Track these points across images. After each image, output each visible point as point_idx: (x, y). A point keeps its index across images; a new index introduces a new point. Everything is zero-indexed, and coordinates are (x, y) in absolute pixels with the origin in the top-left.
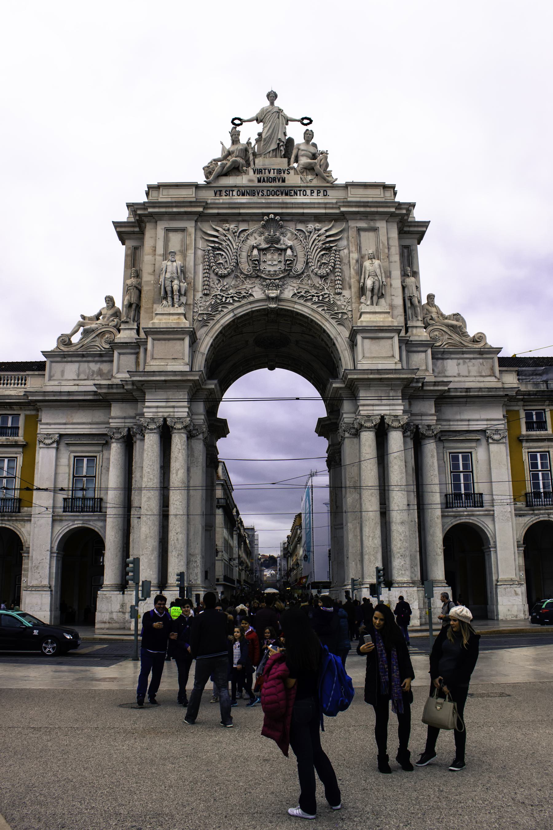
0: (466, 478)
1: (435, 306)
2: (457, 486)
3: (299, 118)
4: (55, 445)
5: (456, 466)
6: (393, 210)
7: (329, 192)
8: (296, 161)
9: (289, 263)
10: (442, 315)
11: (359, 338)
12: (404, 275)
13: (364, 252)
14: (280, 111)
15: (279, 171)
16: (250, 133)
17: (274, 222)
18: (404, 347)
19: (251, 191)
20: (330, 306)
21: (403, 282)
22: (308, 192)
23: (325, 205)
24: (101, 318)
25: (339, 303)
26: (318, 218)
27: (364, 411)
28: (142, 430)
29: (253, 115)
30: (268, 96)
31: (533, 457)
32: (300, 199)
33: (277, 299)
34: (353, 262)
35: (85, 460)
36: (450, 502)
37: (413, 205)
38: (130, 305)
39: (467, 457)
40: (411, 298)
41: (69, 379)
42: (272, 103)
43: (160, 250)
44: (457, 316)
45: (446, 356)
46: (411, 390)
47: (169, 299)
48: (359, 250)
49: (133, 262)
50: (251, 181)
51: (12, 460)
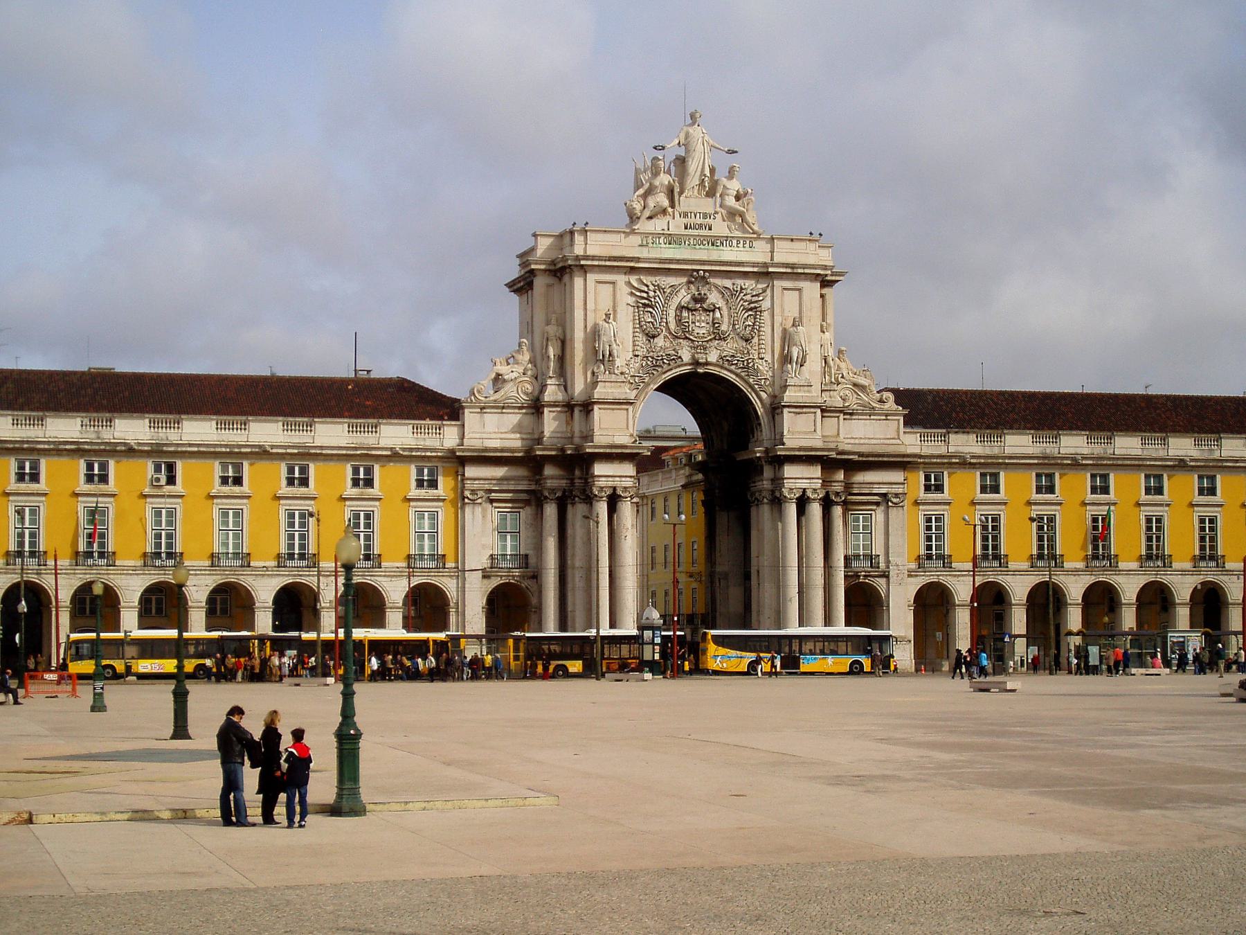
15: (705, 216)
22: (735, 242)
23: (754, 265)
26: (745, 275)
27: (788, 484)
33: (707, 364)
48: (783, 311)
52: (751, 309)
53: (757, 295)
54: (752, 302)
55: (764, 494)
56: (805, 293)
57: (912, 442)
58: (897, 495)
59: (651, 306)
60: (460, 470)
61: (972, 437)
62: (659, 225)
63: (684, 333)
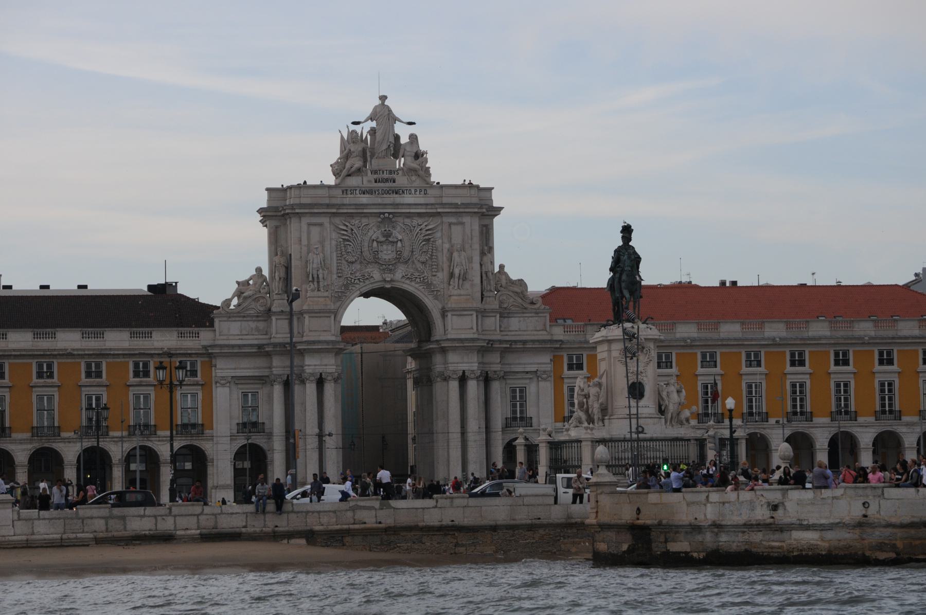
0: (521, 405)
1: (506, 274)
2: (514, 412)
5: (514, 397)
6: (476, 210)
7: (429, 191)
9: (399, 253)
11: (449, 314)
12: (483, 254)
13: (453, 241)
14: (390, 111)
15: (391, 172)
16: (364, 129)
17: (387, 219)
18: (480, 316)
19: (370, 192)
20: (428, 285)
21: (481, 260)
22: (413, 191)
24: (251, 282)
26: (420, 215)
28: (303, 382)
32: (408, 199)
33: (392, 281)
36: (509, 423)
37: (493, 188)
39: (523, 390)
40: (486, 273)
41: (229, 332)
43: (304, 242)
44: (521, 283)
46: (486, 348)
50: (369, 181)
51: (194, 395)
52: (424, 240)
58: (545, 372)
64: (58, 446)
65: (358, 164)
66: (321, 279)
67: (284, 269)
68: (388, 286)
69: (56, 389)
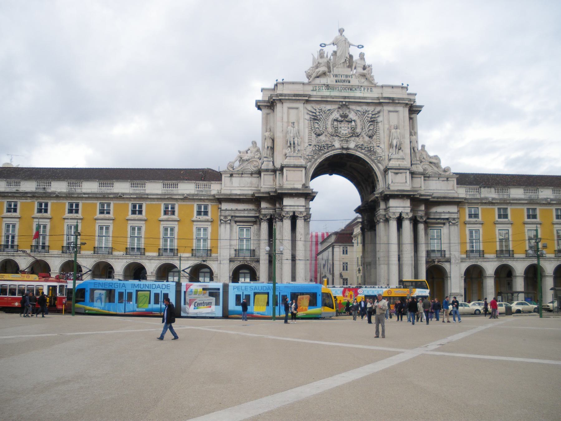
1: (425, 151)
3: (358, 45)
4: (229, 222)
6: (407, 102)
7: (374, 89)
8: (355, 68)
9: (354, 129)
10: (429, 156)
12: (411, 134)
13: (391, 123)
14: (346, 40)
15: (347, 76)
16: (329, 50)
22: (362, 89)
23: (372, 98)
24: (249, 152)
25: (378, 151)
26: (368, 104)
27: (392, 210)
29: (331, 41)
30: (340, 31)
31: (471, 232)
33: (348, 149)
34: (386, 129)
35: (245, 229)
38: (268, 147)
42: (341, 34)
43: (285, 119)
44: (436, 157)
45: (430, 179)
47: (292, 148)
49: (266, 121)
50: (332, 81)
51: (205, 229)
52: (372, 121)
53: (375, 114)
54: (371, 118)
55: (380, 217)
56: (401, 113)
57: (462, 192)
58: (454, 219)
59: (317, 120)
60: (220, 206)
61: (493, 190)
62: (323, 81)
63: (336, 134)
64: (111, 262)
65: (323, 69)
66: (296, 144)
67: (271, 141)
68: (345, 152)
69: (111, 221)
